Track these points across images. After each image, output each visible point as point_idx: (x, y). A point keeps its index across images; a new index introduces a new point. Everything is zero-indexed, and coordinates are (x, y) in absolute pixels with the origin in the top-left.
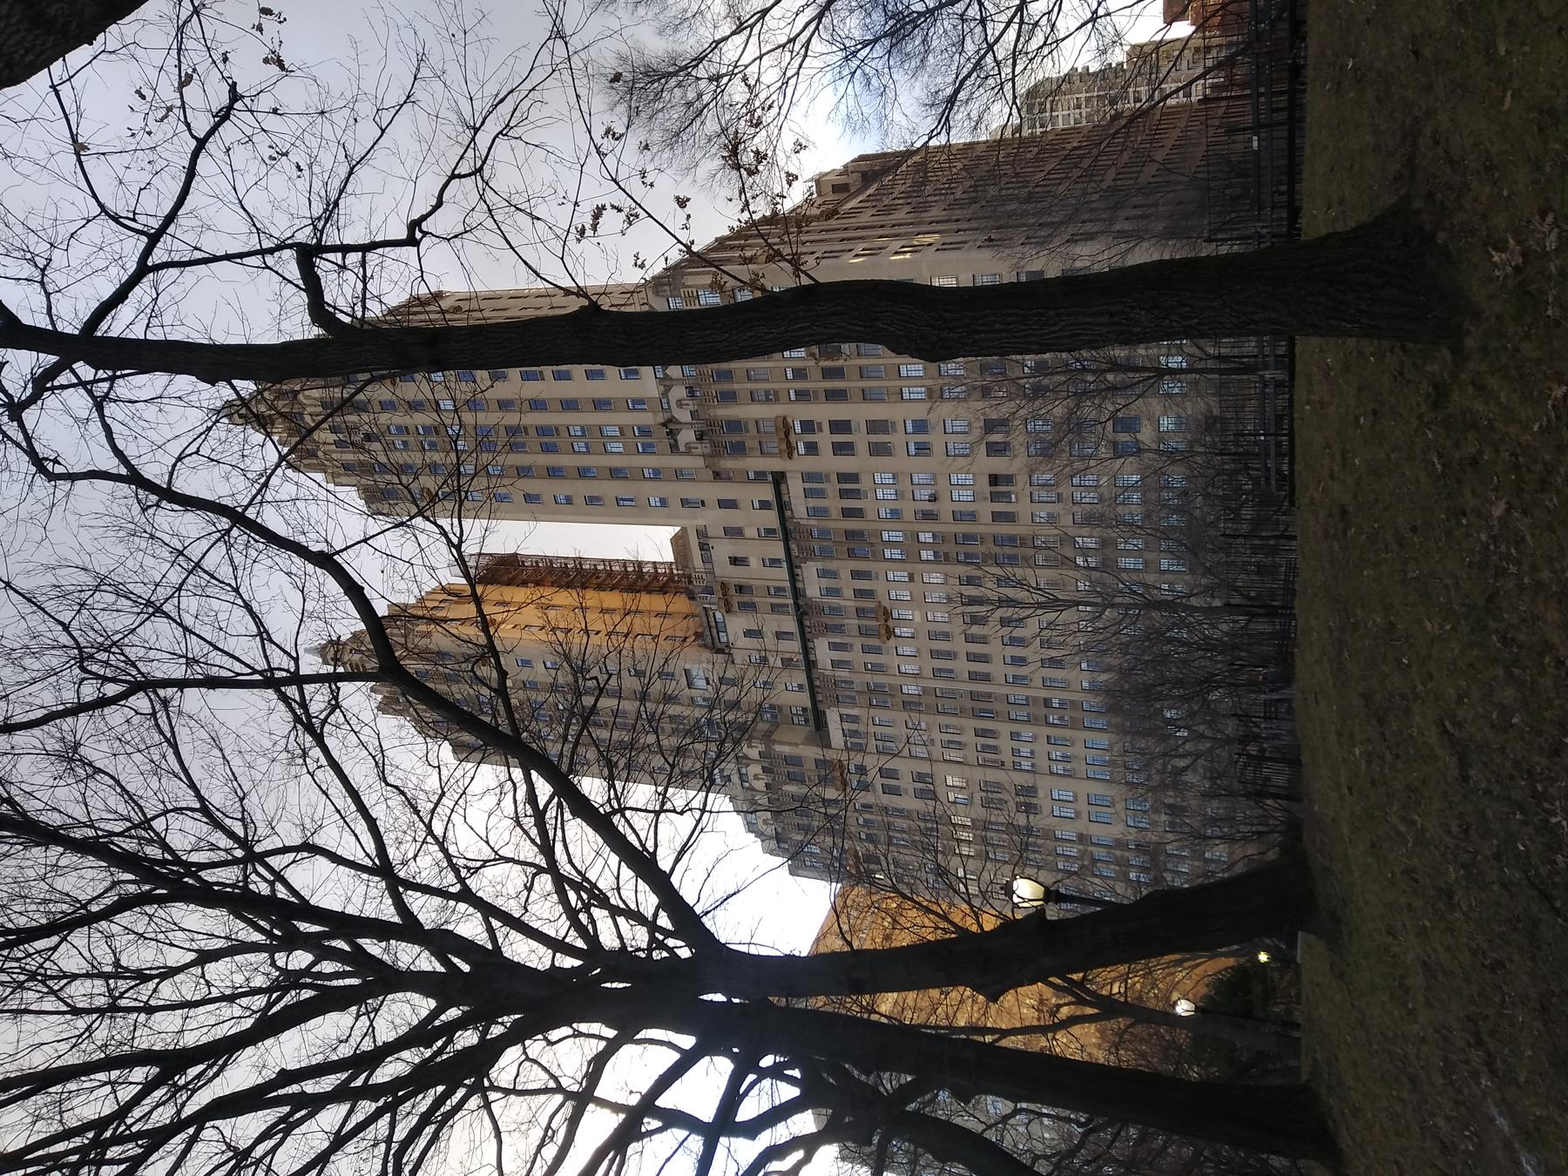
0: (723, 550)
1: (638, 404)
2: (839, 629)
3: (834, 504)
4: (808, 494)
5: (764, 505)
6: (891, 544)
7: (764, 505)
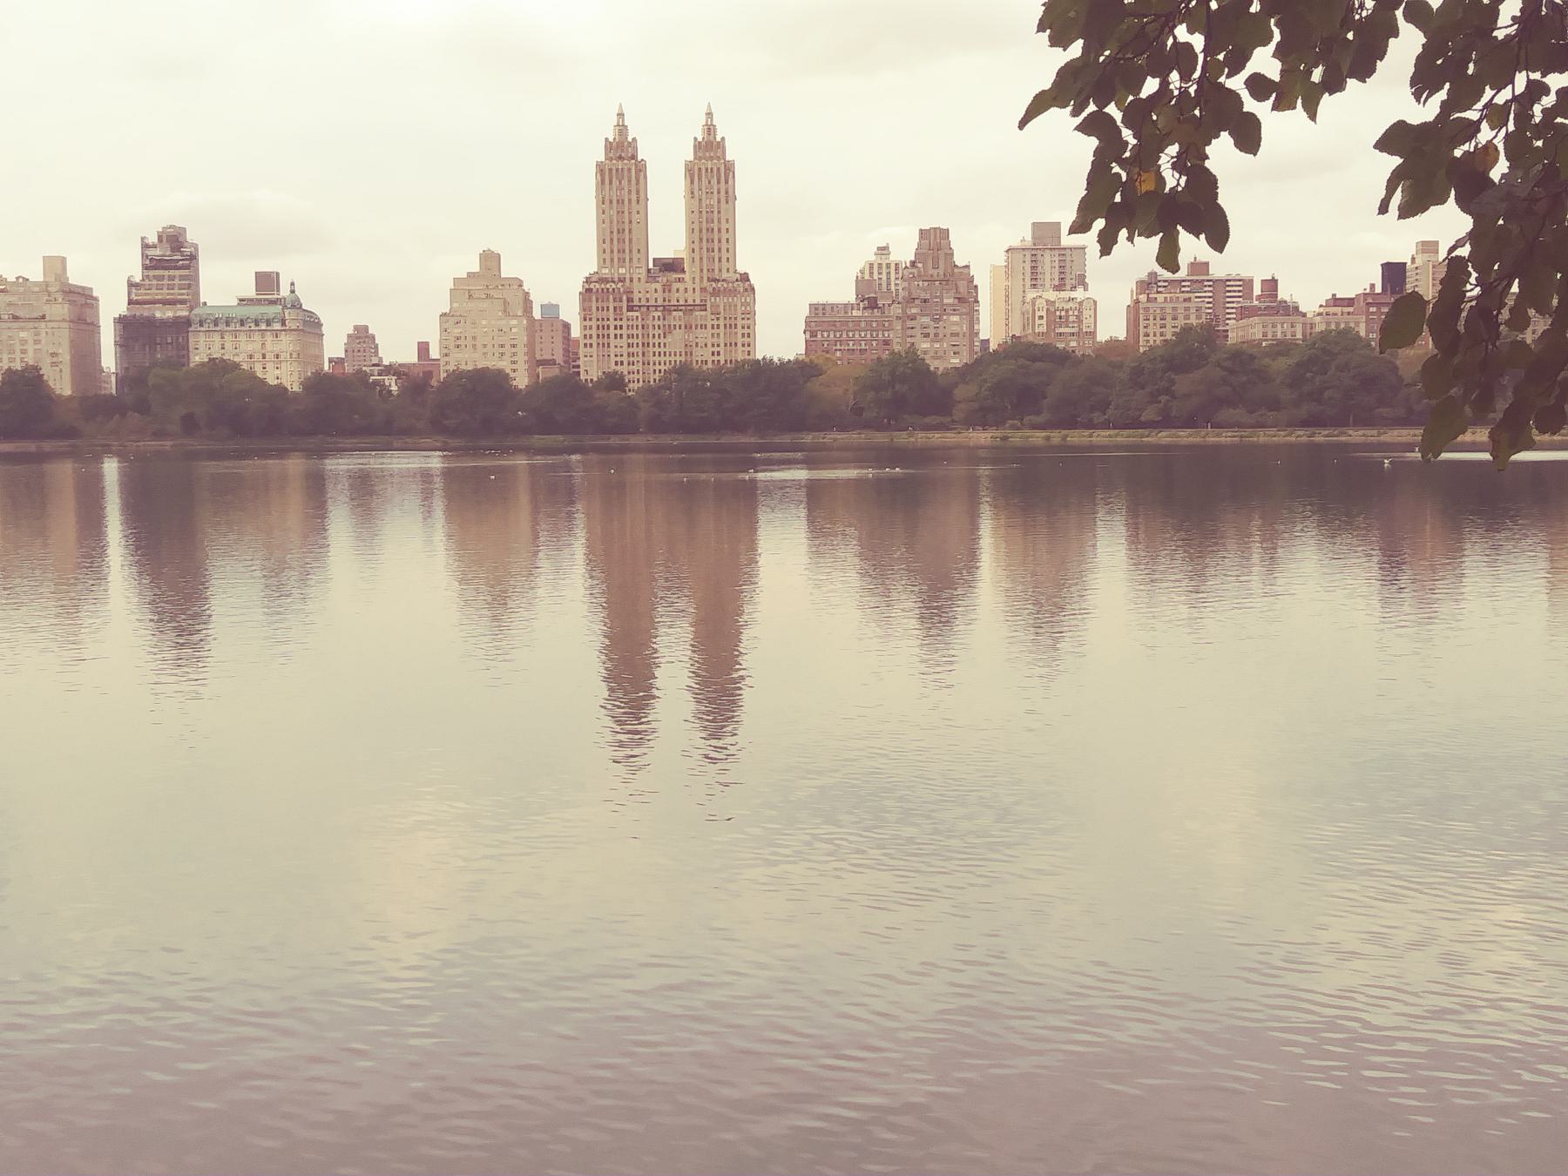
0: (681, 286)
1: (720, 270)
2: (664, 319)
3: (699, 323)
4: (701, 316)
5: (694, 301)
6: (689, 336)
7: (694, 301)
